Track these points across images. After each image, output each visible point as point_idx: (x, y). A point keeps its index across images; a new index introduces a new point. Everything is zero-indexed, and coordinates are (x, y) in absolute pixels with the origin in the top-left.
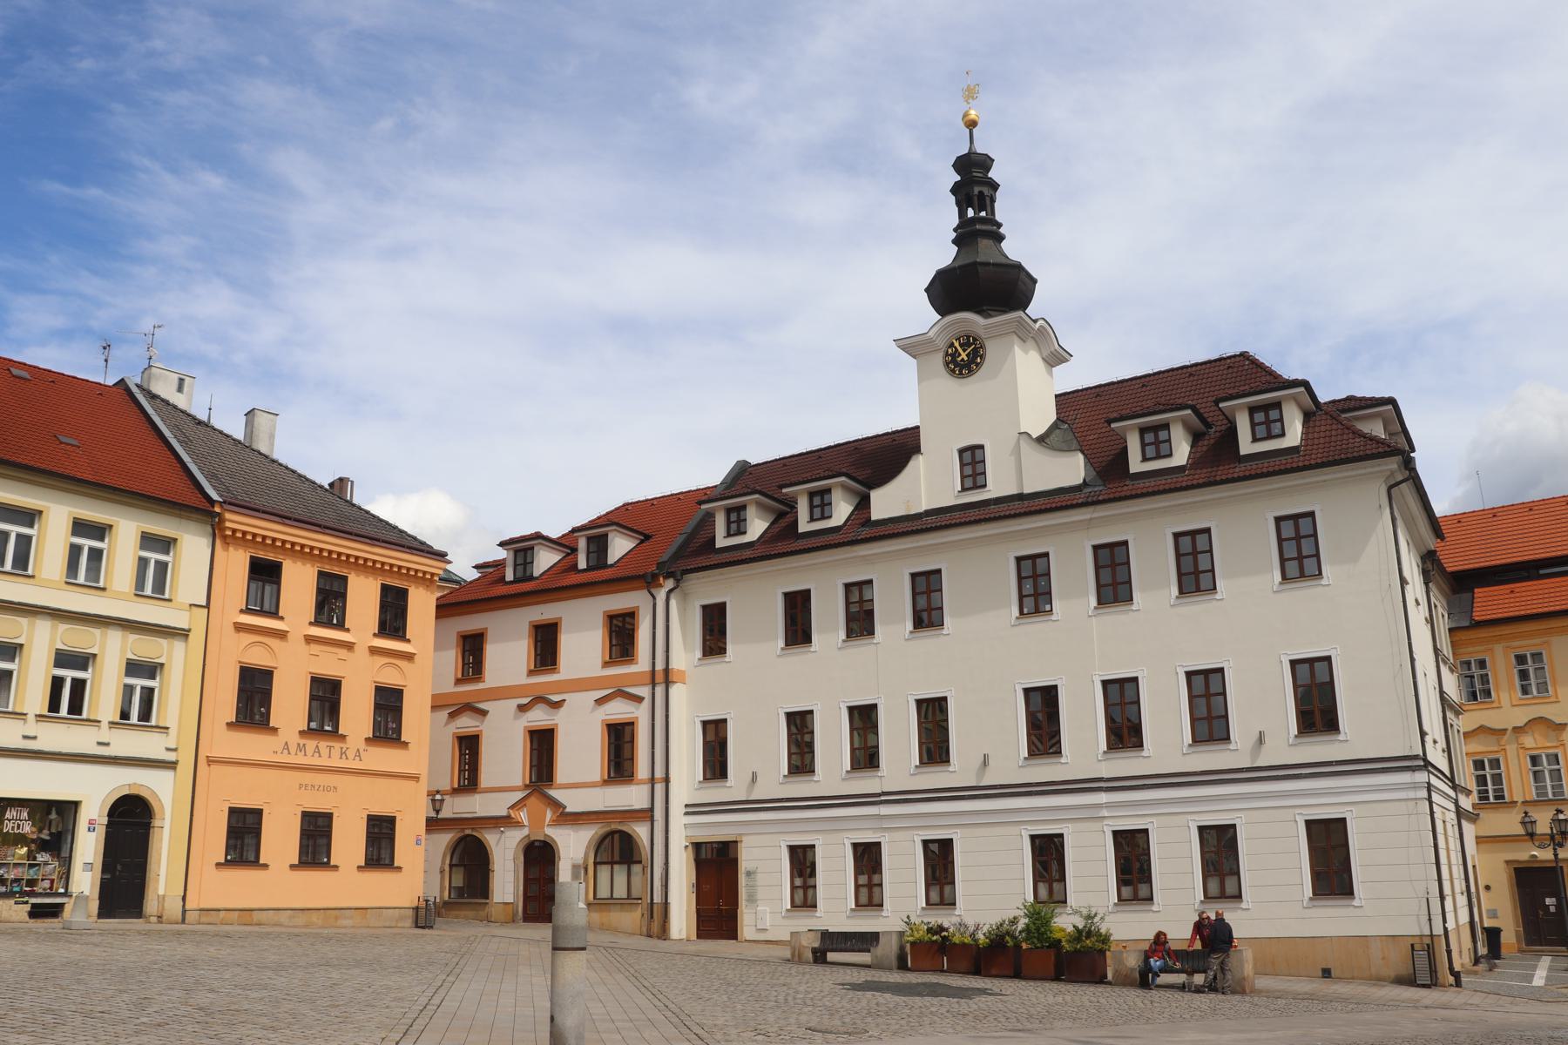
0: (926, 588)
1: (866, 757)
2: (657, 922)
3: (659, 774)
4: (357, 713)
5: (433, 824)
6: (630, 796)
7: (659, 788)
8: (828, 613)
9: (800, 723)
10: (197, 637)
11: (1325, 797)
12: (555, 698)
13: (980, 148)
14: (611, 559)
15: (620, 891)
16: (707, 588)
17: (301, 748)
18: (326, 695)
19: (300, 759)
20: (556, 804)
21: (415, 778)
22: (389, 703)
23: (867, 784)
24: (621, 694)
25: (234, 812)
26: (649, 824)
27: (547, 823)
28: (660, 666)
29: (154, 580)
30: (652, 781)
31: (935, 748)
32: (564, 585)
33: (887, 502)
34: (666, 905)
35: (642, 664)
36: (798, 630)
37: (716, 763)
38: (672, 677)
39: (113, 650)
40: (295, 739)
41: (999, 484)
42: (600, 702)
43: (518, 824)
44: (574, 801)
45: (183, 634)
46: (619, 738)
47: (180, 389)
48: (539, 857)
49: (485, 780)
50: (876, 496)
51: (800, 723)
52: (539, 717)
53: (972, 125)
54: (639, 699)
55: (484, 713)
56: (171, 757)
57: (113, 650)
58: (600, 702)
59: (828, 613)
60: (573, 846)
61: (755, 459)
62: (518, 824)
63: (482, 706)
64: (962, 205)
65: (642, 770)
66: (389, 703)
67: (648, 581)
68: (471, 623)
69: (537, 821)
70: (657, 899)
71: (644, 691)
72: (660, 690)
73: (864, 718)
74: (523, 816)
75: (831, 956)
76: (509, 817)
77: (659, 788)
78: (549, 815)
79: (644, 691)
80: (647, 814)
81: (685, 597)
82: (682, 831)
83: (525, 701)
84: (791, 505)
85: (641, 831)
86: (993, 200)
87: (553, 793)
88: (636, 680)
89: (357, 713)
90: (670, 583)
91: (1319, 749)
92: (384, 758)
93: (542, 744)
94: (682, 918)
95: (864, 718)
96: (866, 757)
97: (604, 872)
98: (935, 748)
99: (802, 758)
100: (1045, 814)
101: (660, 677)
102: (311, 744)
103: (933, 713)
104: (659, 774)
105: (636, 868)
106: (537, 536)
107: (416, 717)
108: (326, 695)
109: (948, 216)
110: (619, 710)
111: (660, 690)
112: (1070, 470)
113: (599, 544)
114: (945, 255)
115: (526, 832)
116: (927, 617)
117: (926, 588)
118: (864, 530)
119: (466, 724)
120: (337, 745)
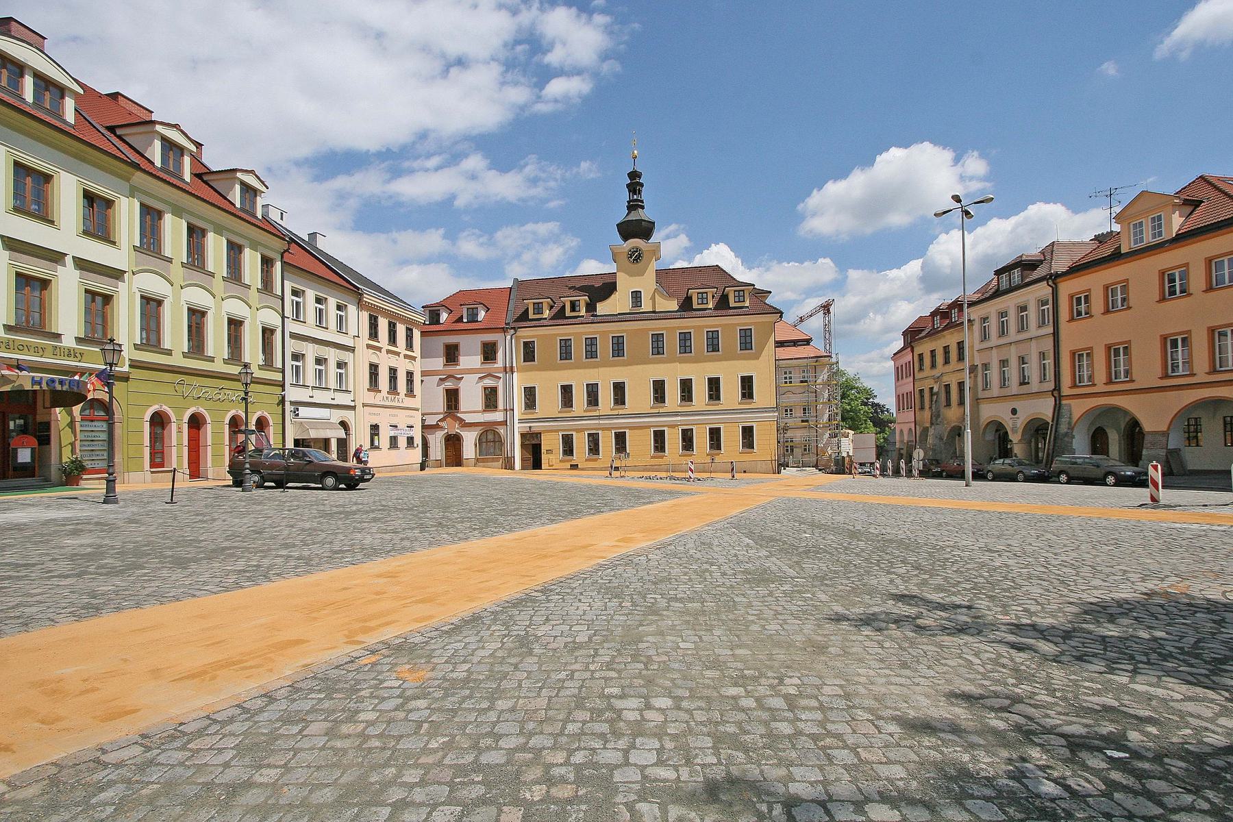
6: (497, 416)
20: (461, 420)
24: (490, 375)
35: (500, 363)
43: (442, 428)
44: (468, 418)
47: (282, 219)
65: (501, 406)
79: (500, 375)
80: (504, 423)
82: (518, 428)
85: (502, 431)
92: (409, 402)
110: (489, 382)
114: (621, 214)
115: (446, 431)
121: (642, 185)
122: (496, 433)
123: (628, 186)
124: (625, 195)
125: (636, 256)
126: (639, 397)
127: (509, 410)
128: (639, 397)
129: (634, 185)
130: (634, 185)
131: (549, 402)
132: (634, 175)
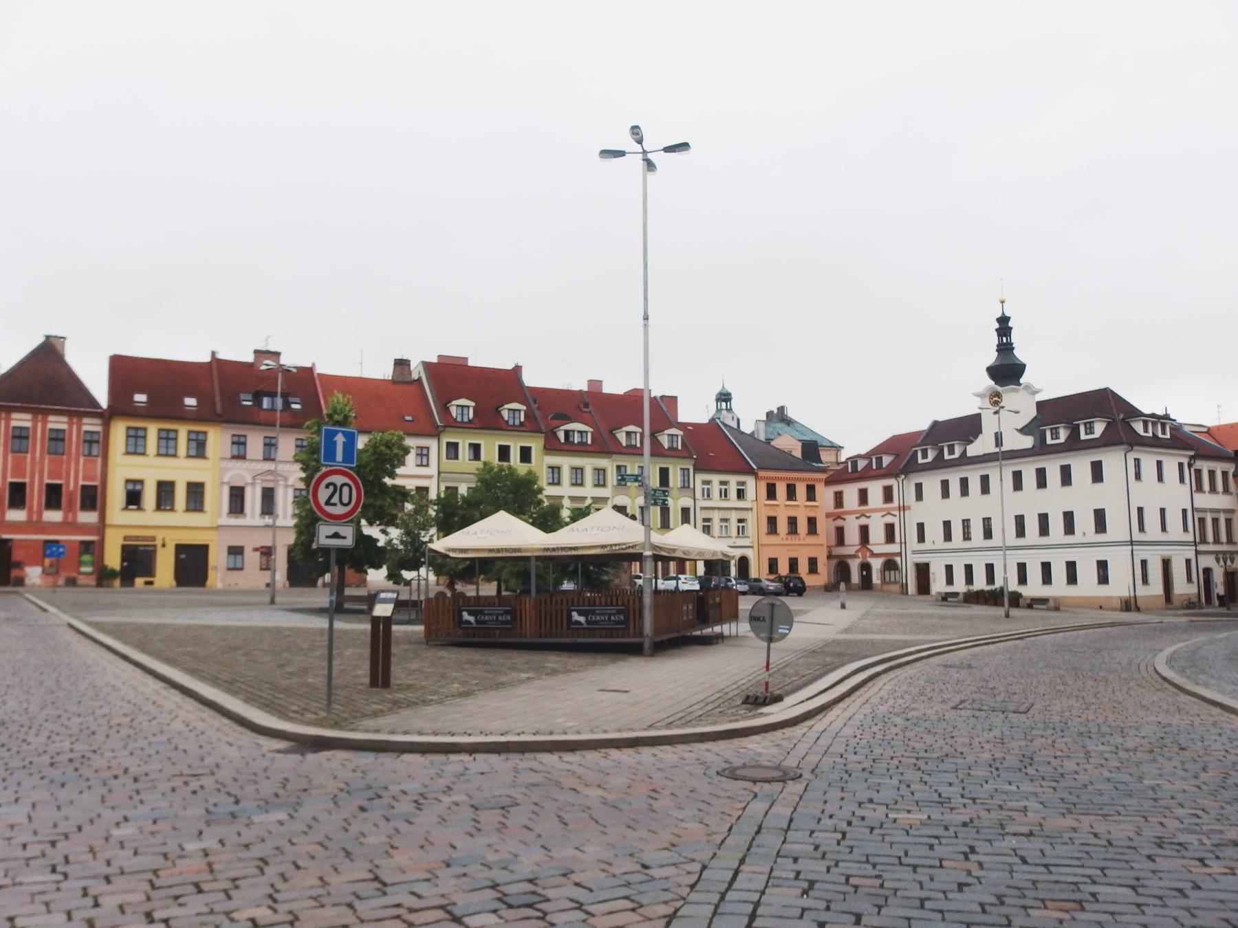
0: (985, 480)
1: (967, 536)
2: (904, 590)
3: (903, 540)
4: (802, 526)
5: (830, 557)
6: (893, 548)
7: (903, 546)
8: (955, 488)
9: (947, 525)
10: (755, 510)
11: (1102, 554)
12: (868, 515)
13: (1007, 314)
14: (884, 466)
15: (893, 579)
17: (787, 539)
18: (792, 522)
19: (787, 543)
20: (870, 550)
21: (822, 545)
22: (812, 522)
23: (967, 545)
25: (770, 559)
28: (902, 504)
29: (741, 494)
31: (988, 534)
32: (867, 475)
33: (973, 450)
34: (907, 584)
35: (895, 504)
36: (945, 493)
37: (921, 538)
39: (734, 517)
40: (784, 537)
41: (1006, 447)
42: (883, 516)
43: (859, 557)
44: (876, 550)
45: (751, 509)
46: (890, 529)
48: (866, 567)
49: (847, 542)
50: (969, 448)
51: (947, 525)
52: (863, 521)
53: (1002, 302)
54: (895, 516)
55: (844, 519)
56: (751, 545)
57: (734, 517)
58: (883, 516)
59: (955, 488)
60: (876, 564)
61: (941, 419)
62: (859, 557)
63: (845, 517)
64: (999, 335)
66: (812, 522)
67: (896, 476)
68: (838, 488)
69: (864, 557)
70: (904, 582)
71: (897, 513)
72: (902, 512)
73: (966, 523)
74: (860, 554)
75: (1034, 606)
77: (903, 546)
78: (868, 554)
80: (900, 554)
81: (909, 480)
83: (858, 515)
84: (942, 450)
85: (898, 559)
86: (1010, 333)
87: (869, 547)
88: (894, 509)
89: (802, 526)
90: (903, 476)
91: (1101, 538)
92: (812, 540)
93: (864, 530)
94: (912, 587)
95: (966, 523)
96: (967, 536)
97: (887, 573)
98: (988, 534)
99: (948, 536)
100: (1021, 556)
101: (902, 509)
102: (789, 537)
103: (987, 522)
104: (903, 540)
105: (897, 572)
106: (859, 456)
107: (822, 525)
108: (792, 522)
109: (994, 340)
110: (889, 519)
111: (902, 512)
112: (1027, 442)
113: (879, 460)
114: (991, 357)
116: (985, 489)
117: (985, 480)
118: (965, 460)
119: (839, 523)
120: (797, 536)
121: (1011, 328)
123: (997, 330)
126: (1004, 530)
127: (904, 543)
128: (1004, 530)
129: (1004, 326)
130: (1004, 326)
131: (934, 533)
132: (1003, 321)
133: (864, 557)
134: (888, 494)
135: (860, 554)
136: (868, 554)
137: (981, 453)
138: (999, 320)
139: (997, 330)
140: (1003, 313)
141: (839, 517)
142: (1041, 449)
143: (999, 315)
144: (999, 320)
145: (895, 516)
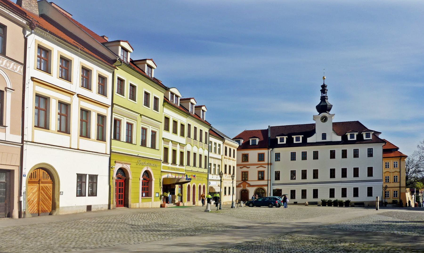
3: (269, 179)
16: (277, 150)
20: (248, 184)
26: (267, 187)
27: (246, 186)
30: (268, 180)
35: (266, 161)
38: (272, 164)
41: (328, 139)
42: (257, 167)
43: (241, 187)
44: (252, 183)
52: (245, 169)
54: (265, 167)
58: (257, 167)
59: (299, 156)
71: (267, 166)
76: (239, 186)
80: (267, 185)
85: (266, 188)
88: (265, 164)
104: (269, 179)
110: (261, 169)
112: (339, 138)
115: (242, 188)
118: (305, 143)
122: (263, 189)
123: (321, 90)
124: (320, 94)
125: (324, 119)
129: (324, 89)
130: (324, 89)
131: (285, 177)
132: (324, 86)
133: (244, 186)
134: (261, 157)
135: (242, 185)
136: (247, 185)
137: (316, 142)
138: (322, 86)
139: (321, 90)
140: (324, 84)
141: (245, 166)
142: (345, 141)
143: (322, 84)
144: (322, 86)
145: (265, 167)
